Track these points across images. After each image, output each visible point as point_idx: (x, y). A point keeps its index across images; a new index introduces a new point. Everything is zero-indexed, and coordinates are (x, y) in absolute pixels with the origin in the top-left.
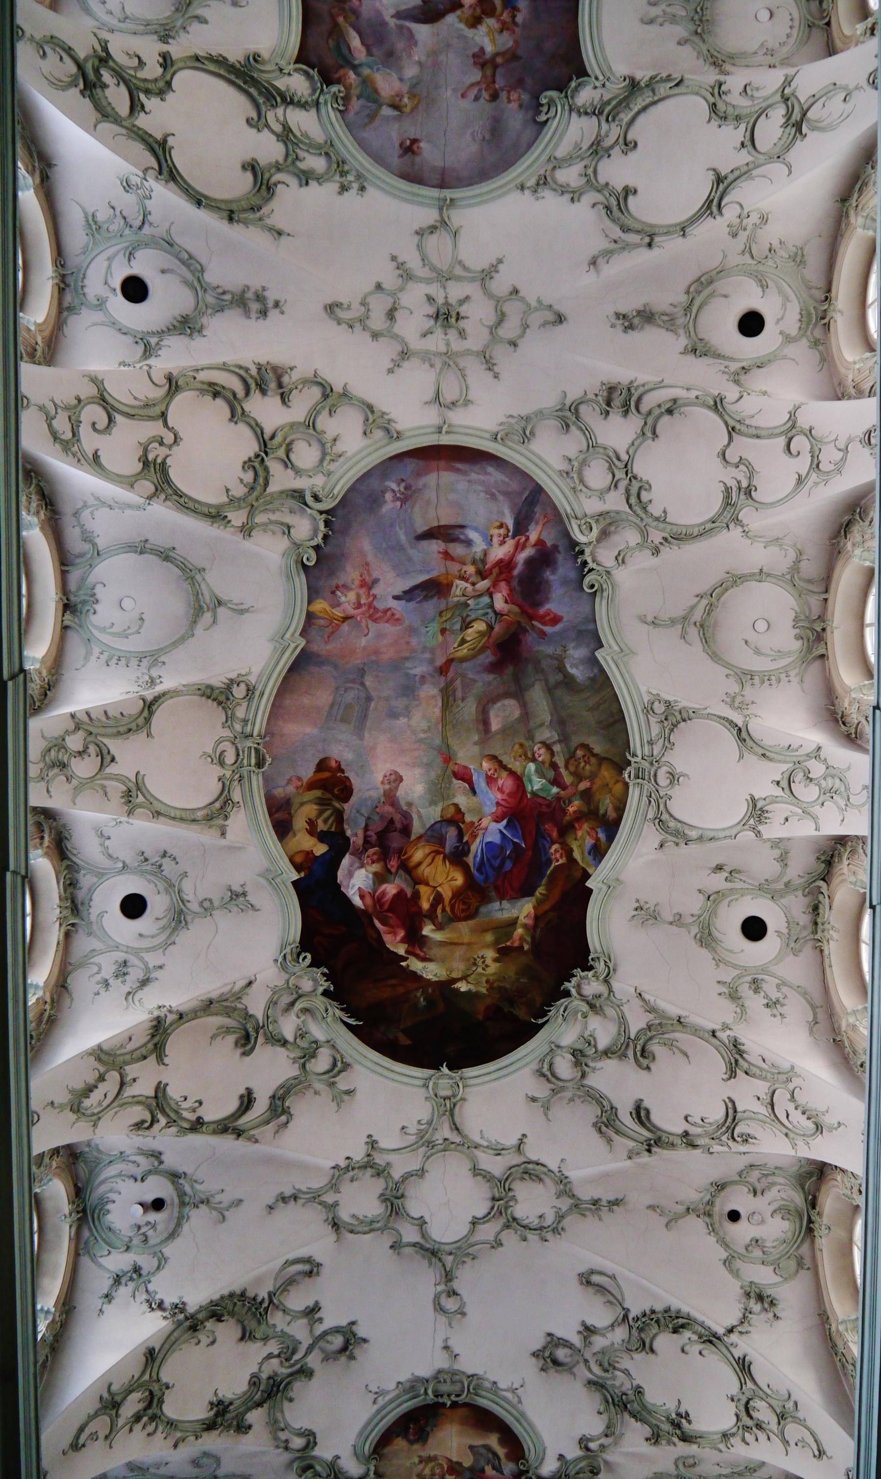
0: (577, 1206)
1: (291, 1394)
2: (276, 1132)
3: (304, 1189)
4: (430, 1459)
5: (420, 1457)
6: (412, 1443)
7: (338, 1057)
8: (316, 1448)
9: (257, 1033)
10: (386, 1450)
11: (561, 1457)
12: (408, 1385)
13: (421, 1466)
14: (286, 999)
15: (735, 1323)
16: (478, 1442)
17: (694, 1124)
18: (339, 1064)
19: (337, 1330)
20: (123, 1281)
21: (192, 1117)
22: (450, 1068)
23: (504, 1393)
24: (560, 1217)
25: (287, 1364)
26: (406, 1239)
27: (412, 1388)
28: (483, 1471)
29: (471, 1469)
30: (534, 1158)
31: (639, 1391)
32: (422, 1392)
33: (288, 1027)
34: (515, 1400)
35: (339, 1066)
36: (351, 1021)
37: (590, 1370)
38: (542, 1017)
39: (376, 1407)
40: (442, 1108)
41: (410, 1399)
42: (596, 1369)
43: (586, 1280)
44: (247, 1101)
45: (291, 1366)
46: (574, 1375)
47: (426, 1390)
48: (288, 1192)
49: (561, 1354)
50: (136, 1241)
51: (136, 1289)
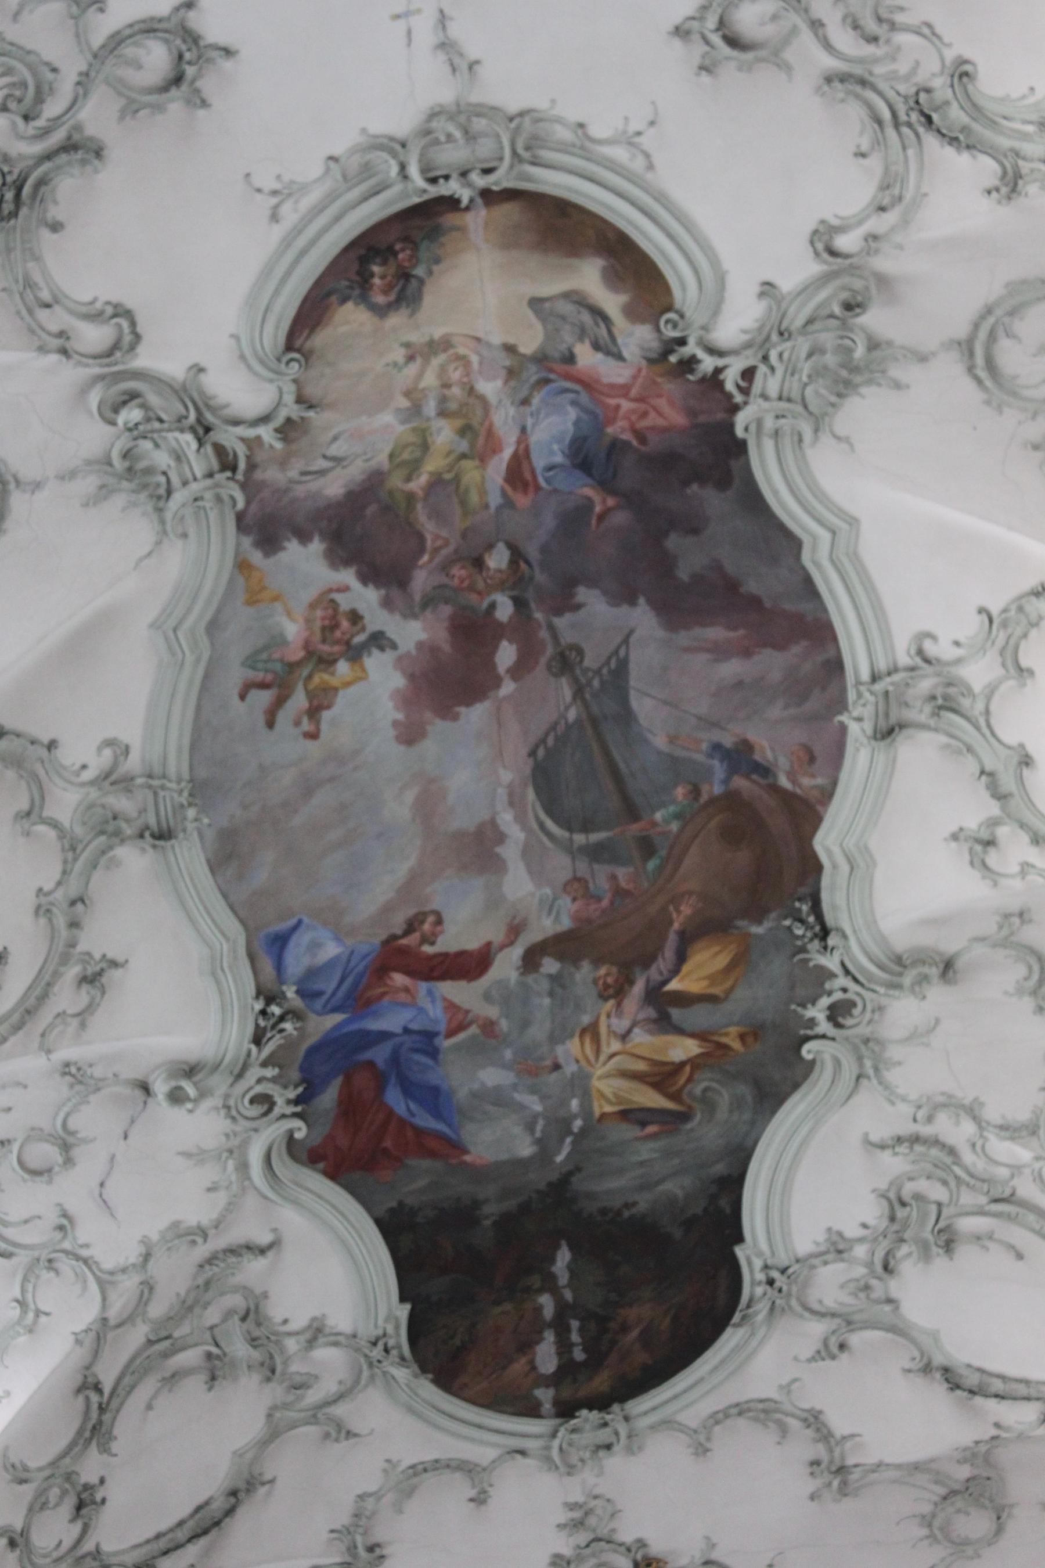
1: (54, 213)
4: (433, 347)
5: (407, 345)
6: (381, 312)
8: (140, 349)
10: (320, 339)
11: (768, 289)
12: (355, 162)
13: (413, 369)
16: (551, 287)
19: (149, 28)
23: (607, 151)
25: (31, 129)
27: (367, 170)
28: (570, 358)
29: (541, 359)
32: (394, 170)
34: (638, 164)
37: (827, 46)
39: (277, 232)
41: (365, 199)
42: (844, 40)
45: (46, 132)
46: (787, 68)
47: (403, 167)
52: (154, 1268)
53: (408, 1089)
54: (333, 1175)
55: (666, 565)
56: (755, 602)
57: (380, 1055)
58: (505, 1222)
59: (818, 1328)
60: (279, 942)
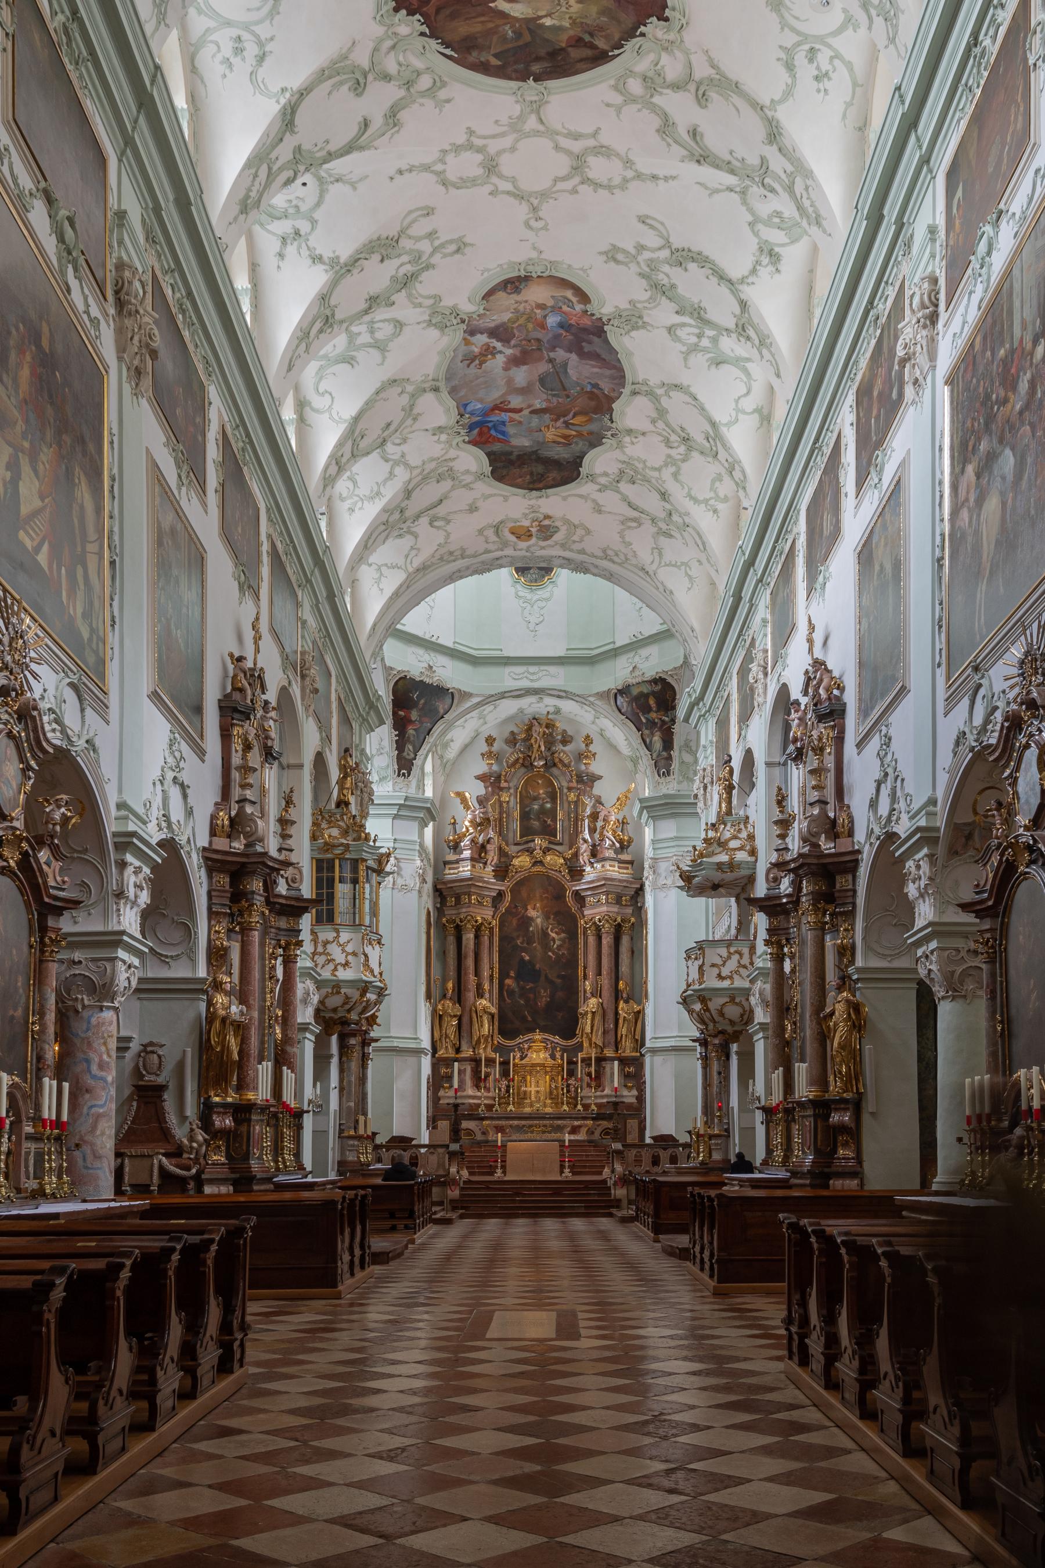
0: (639, 176)
2: (391, 138)
3: (417, 164)
7: (437, 79)
9: (366, 78)
14: (389, 43)
15: (746, 273)
17: (737, 159)
18: (438, 84)
20: (289, 242)
21: (324, 153)
22: (535, 80)
24: (625, 180)
26: (500, 188)
30: (605, 143)
31: (673, 286)
33: (391, 65)
35: (438, 84)
36: (448, 52)
38: (618, 49)
40: (528, 110)
43: (643, 220)
44: (366, 124)
48: (404, 168)
49: (620, 257)
50: (291, 211)
51: (299, 247)
52: (425, 467)
53: (496, 431)
54: (474, 445)
55: (581, 348)
56: (604, 360)
57: (490, 425)
58: (519, 457)
59: (598, 487)
60: (466, 405)
